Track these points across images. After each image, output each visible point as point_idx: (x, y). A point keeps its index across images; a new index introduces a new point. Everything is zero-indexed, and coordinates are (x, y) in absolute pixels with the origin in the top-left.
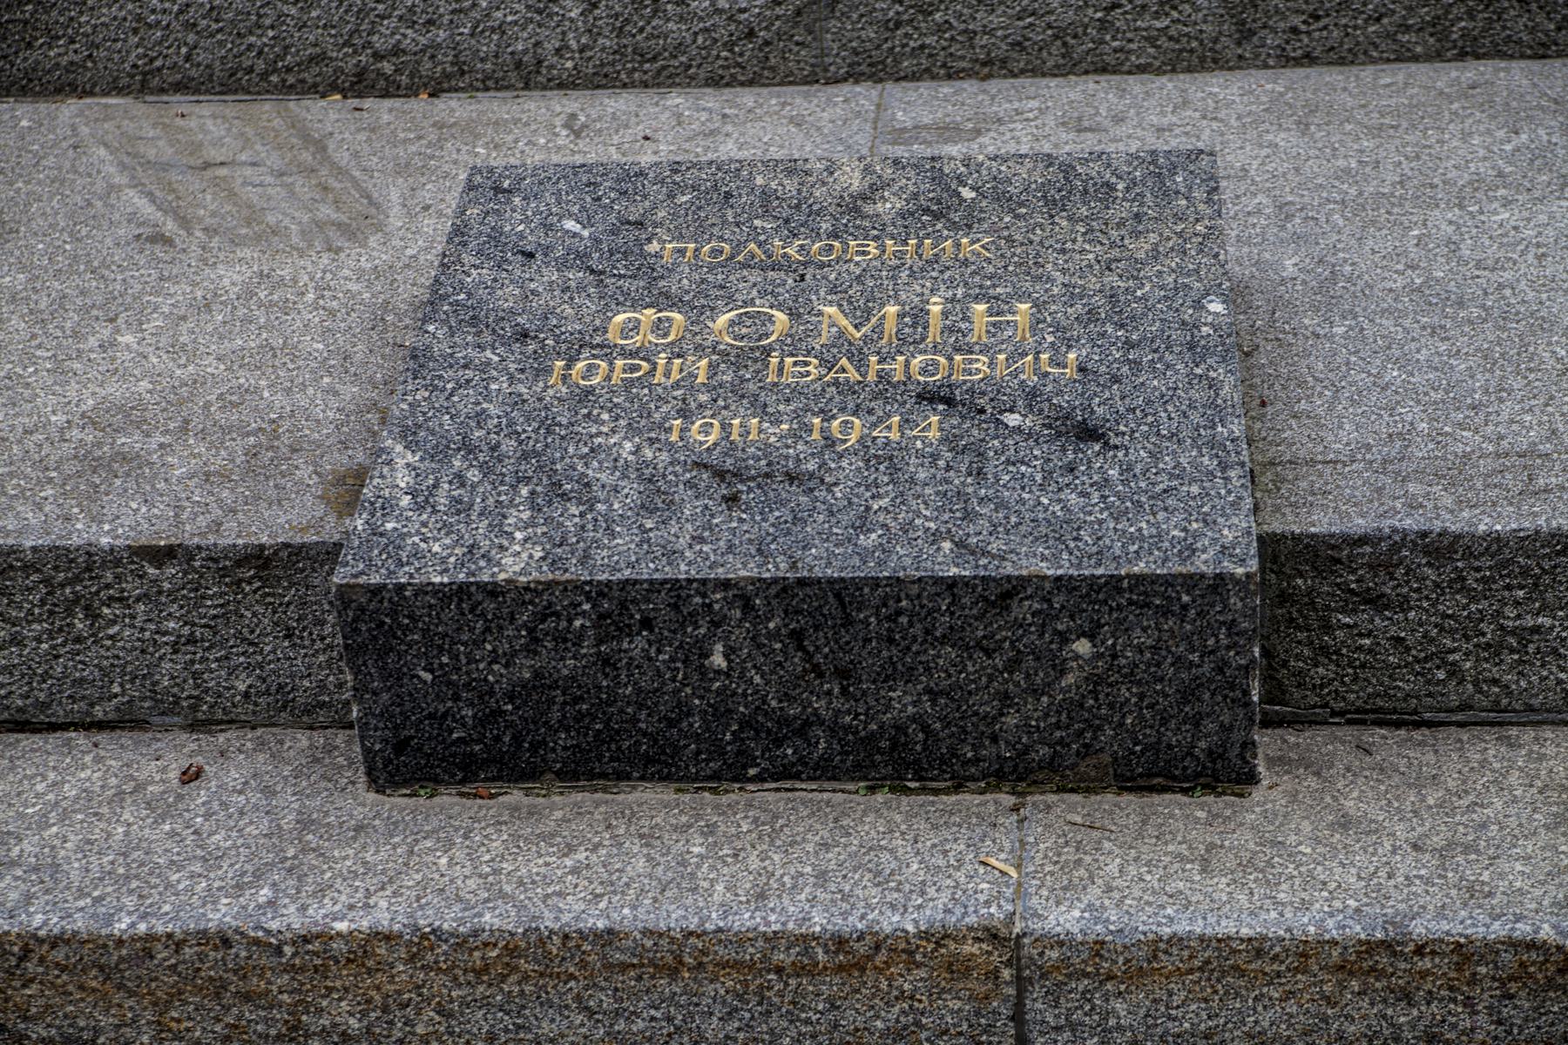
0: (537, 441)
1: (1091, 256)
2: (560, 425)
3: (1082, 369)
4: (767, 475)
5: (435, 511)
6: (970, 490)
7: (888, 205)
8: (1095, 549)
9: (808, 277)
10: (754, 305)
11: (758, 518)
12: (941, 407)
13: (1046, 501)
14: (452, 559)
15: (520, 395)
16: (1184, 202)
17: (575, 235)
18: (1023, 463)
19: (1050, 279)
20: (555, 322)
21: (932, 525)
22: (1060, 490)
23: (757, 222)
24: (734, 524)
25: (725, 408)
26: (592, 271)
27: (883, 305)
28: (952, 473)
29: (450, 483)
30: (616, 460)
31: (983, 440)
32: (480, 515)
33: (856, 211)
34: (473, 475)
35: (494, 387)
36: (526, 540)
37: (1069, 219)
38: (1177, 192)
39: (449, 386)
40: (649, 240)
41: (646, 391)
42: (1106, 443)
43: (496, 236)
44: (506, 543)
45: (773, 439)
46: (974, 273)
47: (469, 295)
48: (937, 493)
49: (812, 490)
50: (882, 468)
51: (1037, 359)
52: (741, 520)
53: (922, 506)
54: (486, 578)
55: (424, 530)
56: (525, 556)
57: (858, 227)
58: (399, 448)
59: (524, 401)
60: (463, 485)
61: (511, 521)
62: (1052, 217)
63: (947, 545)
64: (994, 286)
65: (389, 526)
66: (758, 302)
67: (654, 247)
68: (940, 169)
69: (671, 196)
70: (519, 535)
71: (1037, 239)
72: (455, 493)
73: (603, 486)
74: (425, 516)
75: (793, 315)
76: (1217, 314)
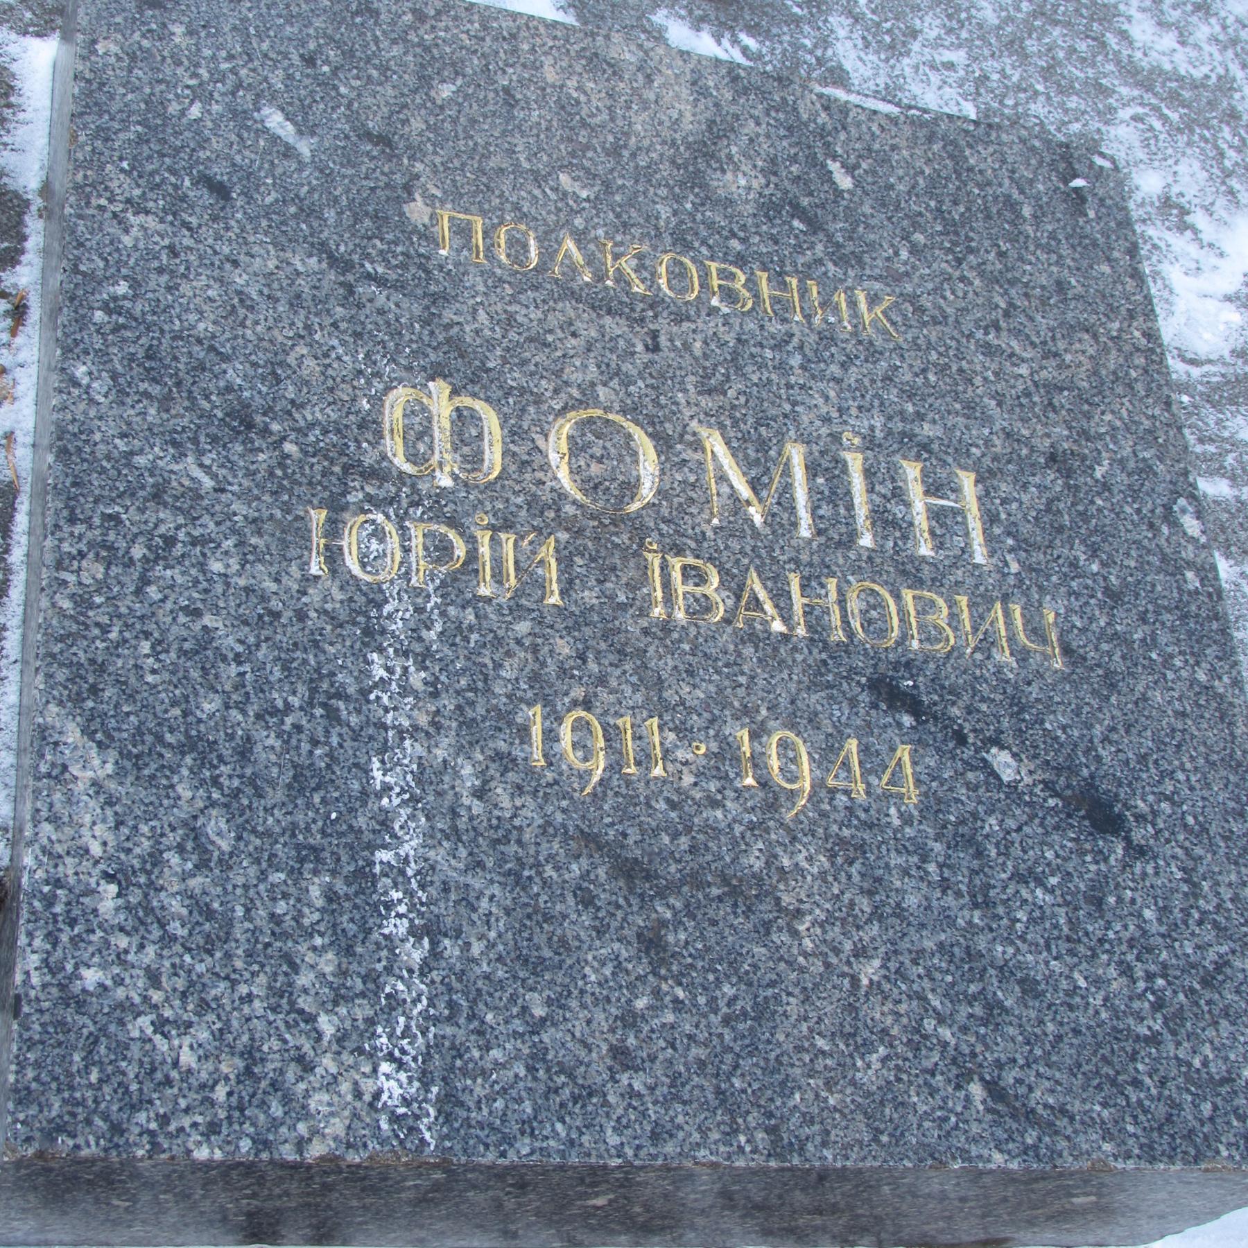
0: (315, 743)
1: (1024, 370)
2: (341, 695)
3: (1067, 651)
4: (696, 880)
5: (168, 940)
6: (982, 943)
7: (743, 182)
8: (1161, 1110)
9: (663, 341)
10: (597, 404)
11: (702, 1000)
12: (907, 720)
13: (1082, 983)
14: (220, 1093)
15: (264, 598)
16: (1105, 268)
17: (288, 152)
18: (1040, 882)
19: (987, 420)
20: (291, 392)
21: (946, 1033)
22: (1094, 956)
23: (564, 178)
24: (669, 1017)
25: (602, 680)
26: (333, 260)
27: (781, 436)
28: (950, 900)
29: (181, 849)
30: (454, 814)
31: (975, 815)
32: (249, 954)
33: (696, 181)
34: (218, 829)
35: (216, 566)
36: (341, 1038)
37: (982, 274)
38: (1095, 244)
39: (138, 552)
40: (408, 188)
41: (470, 617)
42: (1128, 840)
43: (156, 123)
44: (307, 1047)
45: (688, 780)
46: (887, 379)
47: (135, 284)
48: (941, 945)
49: (767, 926)
50: (856, 878)
51: (1007, 614)
52: (677, 1003)
53: (926, 984)
54: (288, 1153)
55: (157, 997)
56: (345, 1087)
57: (710, 225)
58: (73, 734)
59: (276, 615)
60: (203, 865)
61: (304, 979)
62: (959, 262)
63: (976, 1090)
64: (920, 417)
65: (91, 977)
66: (602, 392)
67: (417, 211)
68: (795, 109)
69: (425, 81)
70: (327, 1025)
71: (950, 311)
72: (196, 883)
73: (446, 889)
74: (151, 950)
75: (663, 443)
76: (1193, 540)
